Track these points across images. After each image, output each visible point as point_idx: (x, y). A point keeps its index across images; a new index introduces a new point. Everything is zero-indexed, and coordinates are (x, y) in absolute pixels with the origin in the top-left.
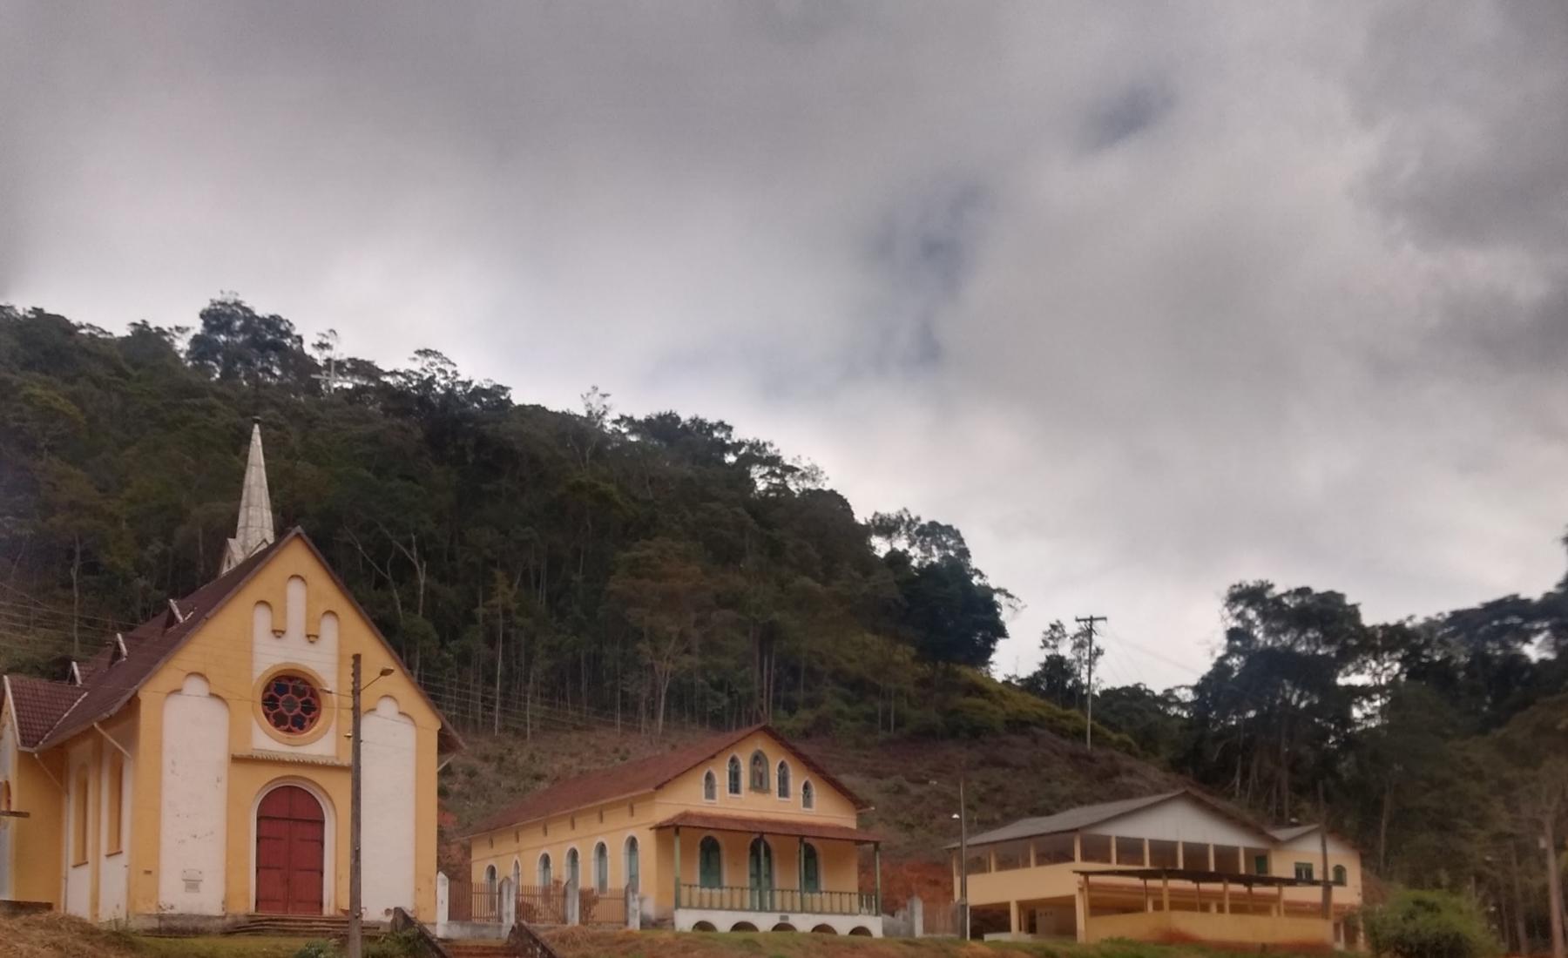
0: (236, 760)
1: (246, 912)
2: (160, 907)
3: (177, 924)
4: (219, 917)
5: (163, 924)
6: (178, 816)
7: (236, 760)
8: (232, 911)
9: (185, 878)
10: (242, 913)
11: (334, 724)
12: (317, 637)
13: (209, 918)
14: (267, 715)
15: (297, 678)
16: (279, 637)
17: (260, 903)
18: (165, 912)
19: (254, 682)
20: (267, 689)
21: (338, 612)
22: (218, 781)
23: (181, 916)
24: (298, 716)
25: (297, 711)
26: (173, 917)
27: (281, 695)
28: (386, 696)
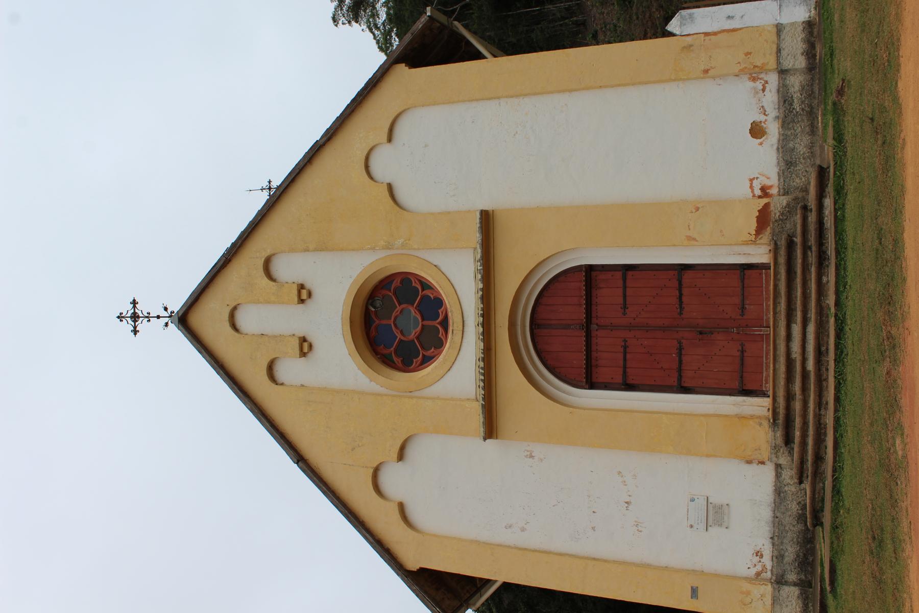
0: (491, 430)
1: (765, 424)
2: (758, 574)
3: (791, 552)
4: (778, 475)
5: (792, 577)
6: (593, 528)
7: (491, 430)
8: (765, 453)
9: (702, 526)
10: (771, 433)
11: (421, 254)
12: (301, 287)
13: (779, 491)
14: (427, 360)
15: (367, 309)
16: (311, 346)
17: (749, 387)
18: (769, 567)
19: (383, 390)
20: (387, 362)
21: (265, 255)
22: (531, 457)
23: (777, 538)
24: (419, 309)
25: (413, 312)
26: (779, 557)
27: (397, 337)
28: (367, 167)
